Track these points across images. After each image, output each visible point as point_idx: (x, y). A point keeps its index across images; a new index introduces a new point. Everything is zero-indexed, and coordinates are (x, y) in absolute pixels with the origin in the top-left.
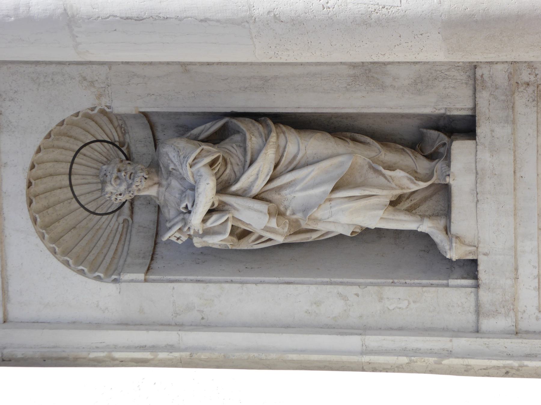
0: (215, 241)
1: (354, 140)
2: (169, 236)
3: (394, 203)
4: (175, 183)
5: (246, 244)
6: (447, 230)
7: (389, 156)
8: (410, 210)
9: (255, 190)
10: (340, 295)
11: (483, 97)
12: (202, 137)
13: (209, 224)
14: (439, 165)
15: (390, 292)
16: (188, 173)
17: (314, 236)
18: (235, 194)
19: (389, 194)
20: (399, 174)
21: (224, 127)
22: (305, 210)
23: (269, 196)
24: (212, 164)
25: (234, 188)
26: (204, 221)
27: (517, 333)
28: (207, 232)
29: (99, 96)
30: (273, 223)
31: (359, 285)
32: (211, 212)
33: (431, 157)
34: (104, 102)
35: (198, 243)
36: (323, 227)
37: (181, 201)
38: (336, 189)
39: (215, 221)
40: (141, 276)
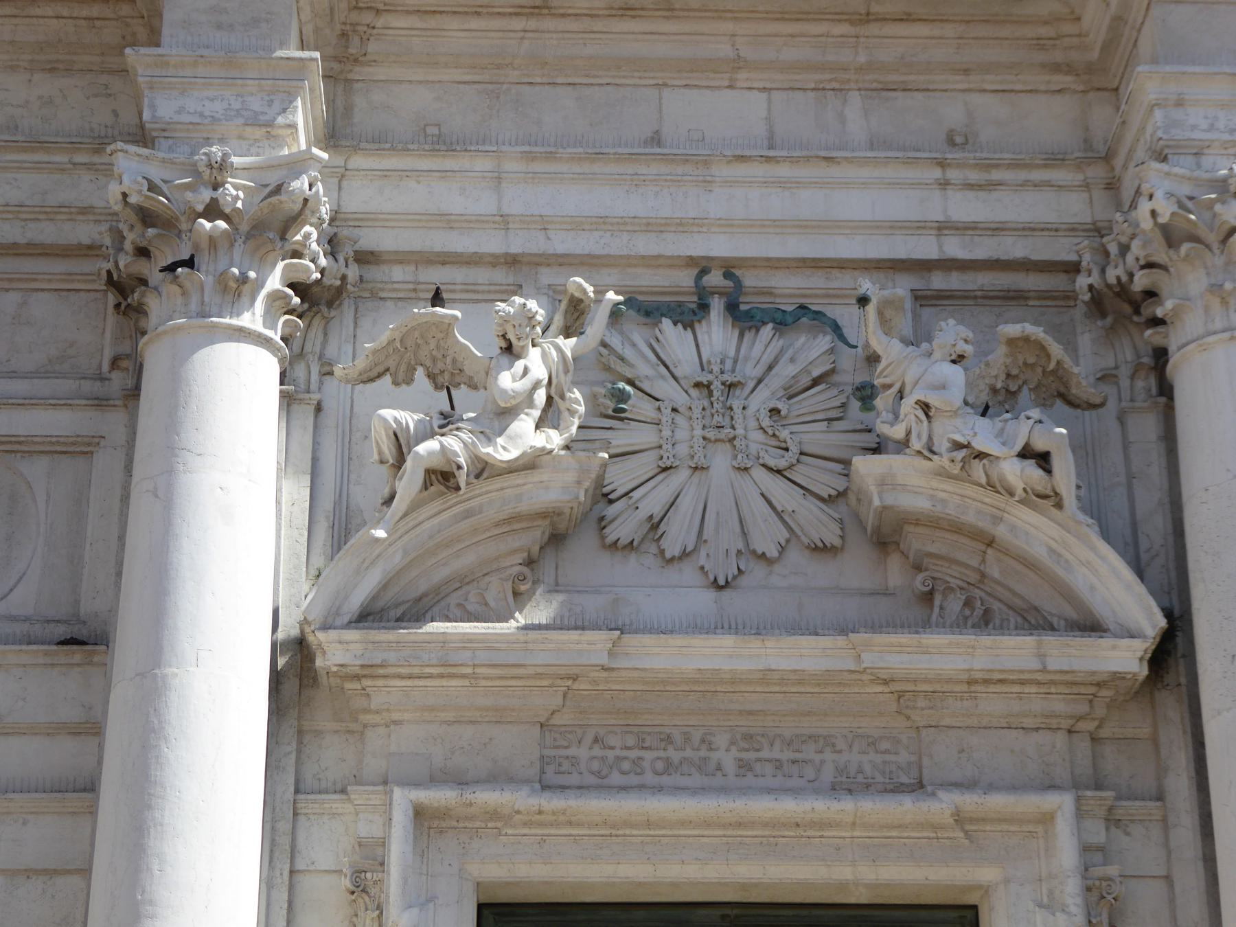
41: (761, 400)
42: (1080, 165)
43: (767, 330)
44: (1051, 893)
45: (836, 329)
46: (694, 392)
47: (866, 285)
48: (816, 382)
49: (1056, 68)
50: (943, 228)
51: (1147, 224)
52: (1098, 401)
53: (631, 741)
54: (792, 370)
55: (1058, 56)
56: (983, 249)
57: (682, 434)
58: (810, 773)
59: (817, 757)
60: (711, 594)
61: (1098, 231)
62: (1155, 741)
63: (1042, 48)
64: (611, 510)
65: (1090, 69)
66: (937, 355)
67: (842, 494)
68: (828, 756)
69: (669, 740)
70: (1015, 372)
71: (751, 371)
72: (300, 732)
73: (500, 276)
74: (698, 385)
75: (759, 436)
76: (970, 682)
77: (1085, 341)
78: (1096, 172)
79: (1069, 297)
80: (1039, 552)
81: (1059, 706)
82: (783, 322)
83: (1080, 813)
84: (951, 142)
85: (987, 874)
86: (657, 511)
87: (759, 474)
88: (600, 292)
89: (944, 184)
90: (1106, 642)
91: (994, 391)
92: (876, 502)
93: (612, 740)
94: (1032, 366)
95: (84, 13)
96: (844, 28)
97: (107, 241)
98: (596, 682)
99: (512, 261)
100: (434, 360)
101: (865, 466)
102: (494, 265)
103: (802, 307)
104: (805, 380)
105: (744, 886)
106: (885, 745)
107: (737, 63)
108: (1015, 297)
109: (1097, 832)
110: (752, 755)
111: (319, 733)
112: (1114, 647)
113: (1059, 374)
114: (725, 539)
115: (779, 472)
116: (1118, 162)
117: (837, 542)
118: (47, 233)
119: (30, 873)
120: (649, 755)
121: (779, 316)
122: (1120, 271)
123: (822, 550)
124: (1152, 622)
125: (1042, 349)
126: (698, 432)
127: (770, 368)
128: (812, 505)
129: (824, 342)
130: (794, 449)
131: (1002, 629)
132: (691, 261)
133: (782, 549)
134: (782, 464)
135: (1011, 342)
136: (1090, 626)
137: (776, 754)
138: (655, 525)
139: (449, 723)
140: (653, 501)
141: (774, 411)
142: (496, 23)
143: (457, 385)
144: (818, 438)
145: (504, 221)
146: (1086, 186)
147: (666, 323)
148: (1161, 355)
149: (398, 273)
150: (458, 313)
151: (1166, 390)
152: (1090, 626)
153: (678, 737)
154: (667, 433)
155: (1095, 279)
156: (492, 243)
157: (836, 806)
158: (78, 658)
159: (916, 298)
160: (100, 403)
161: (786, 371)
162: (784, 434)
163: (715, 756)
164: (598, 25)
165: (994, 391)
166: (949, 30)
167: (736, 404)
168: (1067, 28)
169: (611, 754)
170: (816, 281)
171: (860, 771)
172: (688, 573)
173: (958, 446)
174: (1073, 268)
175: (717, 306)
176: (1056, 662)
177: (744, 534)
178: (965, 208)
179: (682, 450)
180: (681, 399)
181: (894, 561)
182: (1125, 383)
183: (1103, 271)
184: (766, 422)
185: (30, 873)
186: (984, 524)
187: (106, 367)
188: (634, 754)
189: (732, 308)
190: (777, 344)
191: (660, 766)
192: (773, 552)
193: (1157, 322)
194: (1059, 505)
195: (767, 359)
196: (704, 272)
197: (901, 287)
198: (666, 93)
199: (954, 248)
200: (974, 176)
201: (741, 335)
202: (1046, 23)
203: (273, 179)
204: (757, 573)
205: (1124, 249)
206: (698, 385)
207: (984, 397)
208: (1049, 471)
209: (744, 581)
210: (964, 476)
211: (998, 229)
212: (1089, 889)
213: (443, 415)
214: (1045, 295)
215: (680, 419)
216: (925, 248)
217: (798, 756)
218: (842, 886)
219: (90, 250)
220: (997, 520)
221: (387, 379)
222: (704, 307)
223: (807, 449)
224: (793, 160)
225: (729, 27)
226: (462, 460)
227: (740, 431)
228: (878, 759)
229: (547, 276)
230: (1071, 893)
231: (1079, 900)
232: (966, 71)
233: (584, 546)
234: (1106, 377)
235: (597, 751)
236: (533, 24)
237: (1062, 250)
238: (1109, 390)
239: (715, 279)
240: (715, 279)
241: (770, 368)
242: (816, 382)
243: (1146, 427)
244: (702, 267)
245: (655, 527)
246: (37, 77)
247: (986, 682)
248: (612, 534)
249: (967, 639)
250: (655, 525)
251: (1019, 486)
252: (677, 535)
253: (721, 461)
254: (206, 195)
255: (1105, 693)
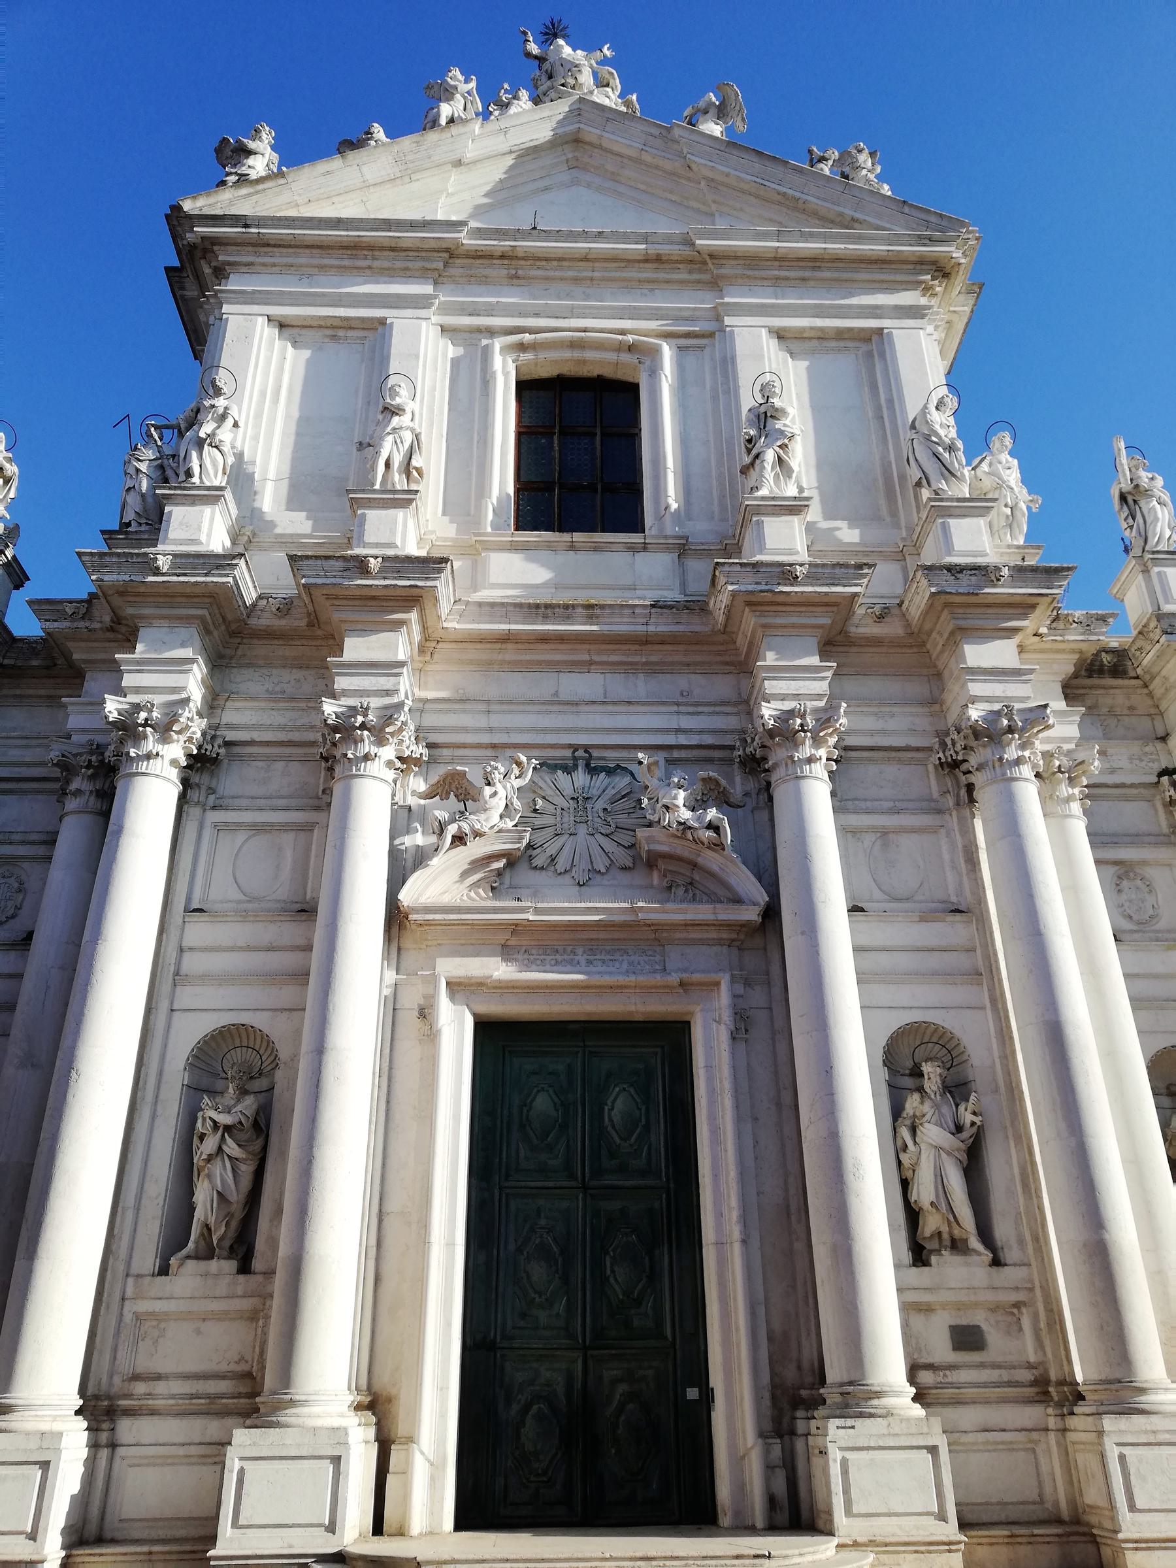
0: (199, 1124)
1: (246, 1203)
2: (206, 1099)
3: (207, 1227)
4: (232, 1102)
5: (196, 1140)
6: (188, 1257)
7: (234, 1224)
8: (202, 1234)
9: (225, 1148)
10: (159, 1194)
11: (259, 1278)
12: (258, 1118)
13: (208, 1120)
14: (225, 1253)
15: (157, 1223)
16: (239, 1108)
17: (195, 1179)
18: (223, 1136)
19: (212, 1221)
20: (223, 1229)
21: (262, 1130)
22: (209, 1176)
23: (220, 1154)
24: (240, 1123)
25: (226, 1134)
26: (210, 1118)
27: (123, 1299)
28: (204, 1119)
29: (285, 1063)
30: (204, 1157)
31: (164, 1206)
32: (215, 1122)
33: (231, 1247)
34: (281, 1066)
35: (200, 1114)
36: (199, 1185)
37: (222, 1105)
38: (218, 1192)
39: (209, 1123)
40: (185, 1083)
41: (600, 805)
42: (736, 704)
43: (603, 775)
44: (720, 1015)
45: (632, 774)
46: (571, 802)
47: (640, 755)
48: (623, 797)
49: (727, 663)
50: (678, 731)
51: (761, 729)
52: (741, 804)
53: (541, 951)
54: (613, 792)
55: (727, 659)
56: (694, 740)
57: (565, 820)
58: (617, 964)
59: (621, 958)
60: (577, 888)
61: (744, 731)
62: (765, 949)
63: (720, 655)
64: (535, 853)
65: (740, 663)
66: (672, 785)
67: (633, 845)
68: (625, 957)
69: (557, 951)
70: (705, 792)
71: (595, 792)
72: (399, 949)
73: (489, 753)
74: (573, 798)
75: (599, 820)
76: (686, 925)
77: (738, 779)
78: (742, 707)
79: (732, 760)
80: (715, 868)
81: (725, 935)
82: (610, 772)
83: (733, 980)
84: (682, 694)
85: (690, 1008)
86: (554, 852)
87: (598, 836)
88: (529, 759)
89: (678, 713)
90: (744, 907)
91: (697, 800)
92: (646, 848)
93: (534, 952)
94: (713, 790)
95: (314, 644)
96: (637, 647)
97: (321, 740)
98: (525, 926)
99: (494, 746)
100: (457, 788)
101: (641, 833)
102: (486, 748)
103: (618, 765)
104: (619, 796)
105: (589, 1014)
106: (650, 953)
107: (591, 663)
108: (710, 760)
109: (740, 989)
110: (592, 958)
111: (407, 949)
112: (747, 910)
113: (724, 792)
114: (584, 865)
115: (607, 835)
116: (752, 703)
117: (631, 865)
118: (296, 736)
119: (282, 1010)
120: (549, 958)
121: (607, 769)
122: (751, 749)
123: (625, 869)
124: (763, 897)
125: (718, 783)
126: (572, 818)
127: (604, 791)
128: (621, 849)
129: (627, 779)
130: (613, 826)
131: (701, 902)
132: (570, 746)
133: (608, 869)
134: (608, 832)
135: (703, 780)
136: (738, 900)
137: (603, 957)
138: (553, 859)
139: (463, 945)
140: (552, 849)
141: (605, 809)
142: (488, 646)
143: (468, 800)
144: (623, 820)
145: (490, 730)
146: (738, 714)
147: (559, 772)
148: (769, 784)
149: (445, 752)
150: (467, 770)
151: (771, 799)
152: (738, 900)
153: (561, 951)
154: (559, 819)
155: (741, 753)
156: (486, 739)
157: (627, 979)
158: (303, 918)
159: (667, 761)
160: (317, 808)
161: (611, 792)
162: (609, 819)
163: (577, 958)
164: (532, 646)
165: (697, 800)
166: (681, 648)
167: (589, 806)
168: (731, 646)
169: (532, 958)
170: (624, 754)
171: (639, 964)
172: (567, 879)
173: (680, 823)
174: (732, 748)
175: (581, 763)
176: (721, 917)
177: (592, 863)
178: (686, 722)
179: (565, 826)
180: (565, 805)
181: (655, 874)
182: (754, 796)
183: (744, 750)
184: (601, 814)
185: (282, 1010)
186: (692, 857)
187: (320, 793)
188: (542, 957)
189: (587, 765)
190: (607, 780)
191: (553, 962)
192: (603, 870)
193: (767, 771)
194: (723, 849)
195: (603, 787)
196: (576, 750)
197: (660, 756)
198: (561, 674)
199: (683, 740)
200: (691, 709)
201: (592, 777)
202: (722, 644)
203: (389, 713)
204: (598, 877)
205: (753, 740)
206: (573, 798)
207: (693, 803)
208: (719, 834)
209: (590, 882)
210: (683, 837)
211: (701, 732)
212: (736, 1014)
213: (461, 813)
214: (720, 759)
215: (564, 812)
216: (670, 740)
217: (612, 957)
218: (631, 1013)
219: (313, 744)
220: (699, 855)
221: (438, 797)
222: (576, 767)
223: (619, 825)
224: (614, 703)
225: (587, 646)
226: (467, 832)
227: (590, 818)
228: (646, 958)
229: (509, 753)
230: (726, 1015)
231: (731, 1018)
232: (688, 665)
233: (523, 867)
234: (747, 794)
235: (526, 956)
236: (504, 646)
237: (728, 740)
238: (747, 799)
239: (580, 753)
240: (580, 753)
241: (604, 791)
242: (623, 797)
243: (765, 815)
244: (575, 748)
245: (553, 860)
246: (294, 671)
247: (693, 925)
248: (535, 862)
249: (684, 906)
250: (553, 859)
251: (706, 842)
252: (562, 864)
253: (582, 830)
254: (360, 719)
255: (744, 929)
